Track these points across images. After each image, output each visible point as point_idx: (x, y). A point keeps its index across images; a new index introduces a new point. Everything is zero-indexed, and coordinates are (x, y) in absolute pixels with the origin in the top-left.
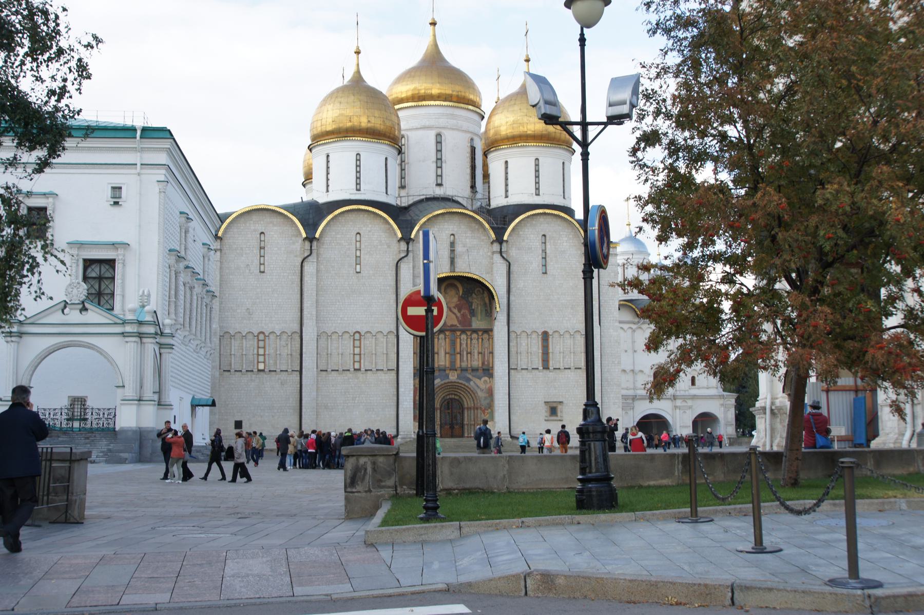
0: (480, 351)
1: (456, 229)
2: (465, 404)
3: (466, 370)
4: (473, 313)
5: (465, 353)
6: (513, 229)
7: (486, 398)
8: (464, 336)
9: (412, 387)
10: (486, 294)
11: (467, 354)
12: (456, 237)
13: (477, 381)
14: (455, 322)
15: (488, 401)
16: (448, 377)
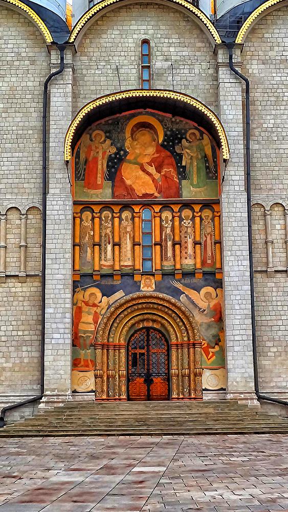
0: (198, 239)
1: (151, 32)
2: (173, 337)
3: (172, 274)
4: (183, 173)
5: (170, 244)
6: (253, 30)
7: (209, 326)
8: (167, 214)
9: (69, 306)
10: (206, 139)
11: (174, 245)
12: (152, 44)
13: (193, 294)
14: (151, 190)
15: (213, 331)
16: (139, 290)
